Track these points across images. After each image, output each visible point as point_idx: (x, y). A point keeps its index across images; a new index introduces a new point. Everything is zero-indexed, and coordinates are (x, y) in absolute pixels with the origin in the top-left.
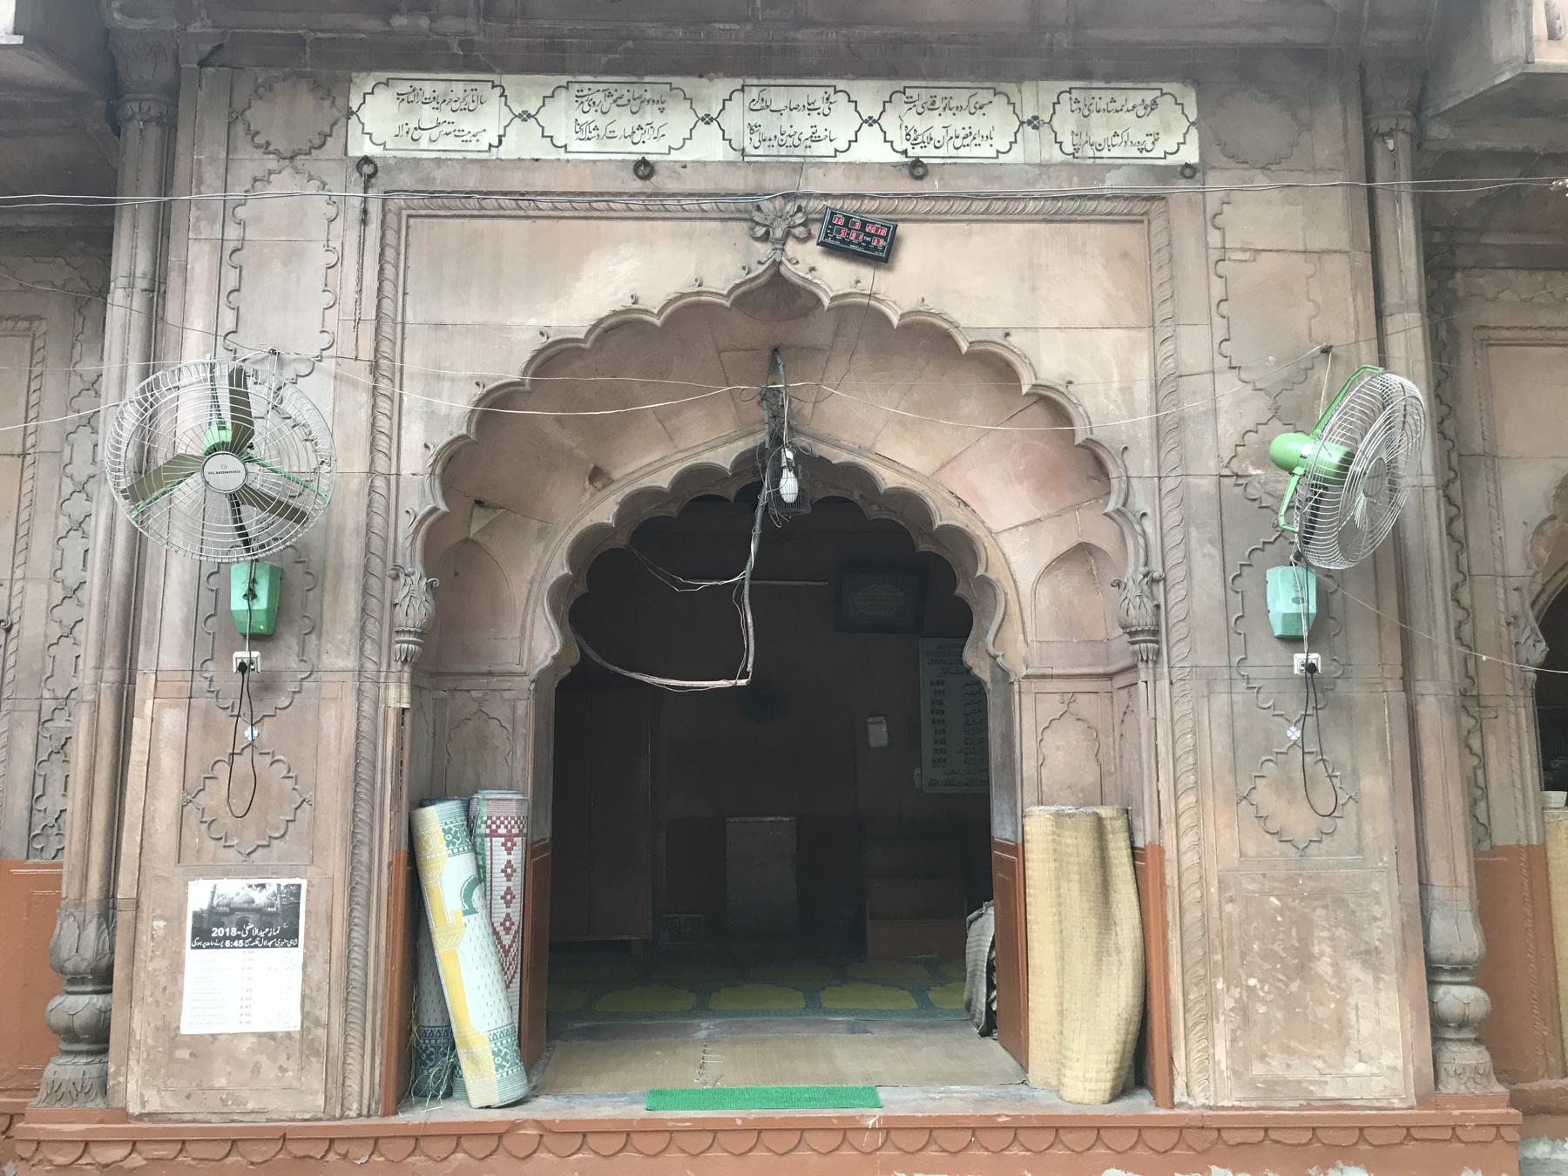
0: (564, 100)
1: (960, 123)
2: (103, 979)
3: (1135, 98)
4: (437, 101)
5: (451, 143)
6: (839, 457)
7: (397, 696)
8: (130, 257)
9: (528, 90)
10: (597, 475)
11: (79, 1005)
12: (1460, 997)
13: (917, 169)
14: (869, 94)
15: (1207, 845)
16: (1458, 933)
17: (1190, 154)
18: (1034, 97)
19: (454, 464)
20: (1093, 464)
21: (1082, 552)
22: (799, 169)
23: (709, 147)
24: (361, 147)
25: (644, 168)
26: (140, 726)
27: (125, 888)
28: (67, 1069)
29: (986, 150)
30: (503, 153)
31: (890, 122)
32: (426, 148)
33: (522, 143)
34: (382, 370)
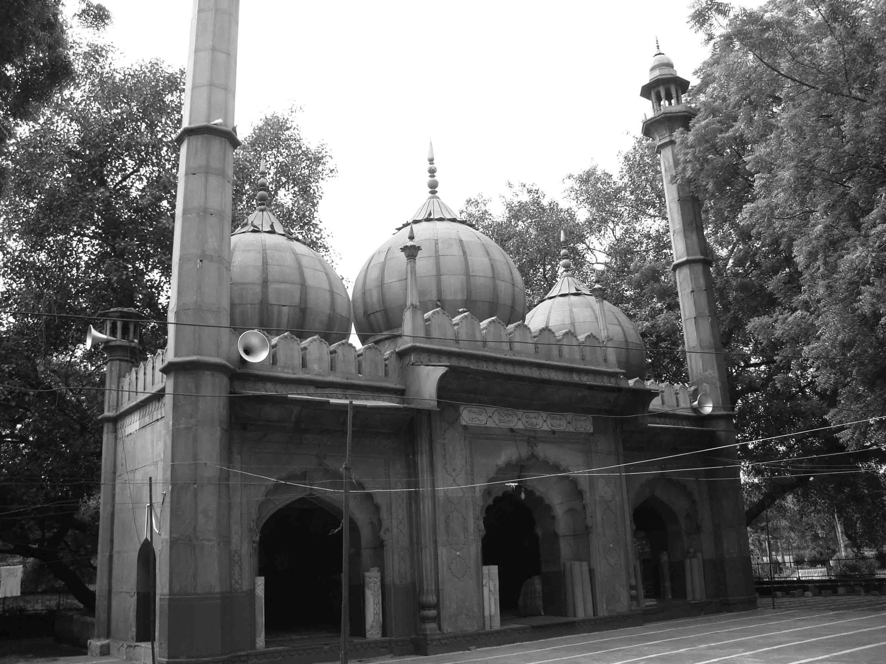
0: (496, 413)
2: (436, 606)
3: (583, 418)
4: (475, 413)
5: (478, 422)
6: (529, 489)
8: (425, 447)
13: (554, 432)
14: (544, 415)
15: (601, 567)
17: (591, 431)
20: (580, 494)
21: (571, 511)
22: (535, 431)
23: (520, 426)
24: (464, 423)
25: (512, 430)
26: (439, 553)
27: (440, 587)
28: (434, 625)
29: (562, 428)
30: (488, 425)
31: (549, 422)
33: (490, 424)
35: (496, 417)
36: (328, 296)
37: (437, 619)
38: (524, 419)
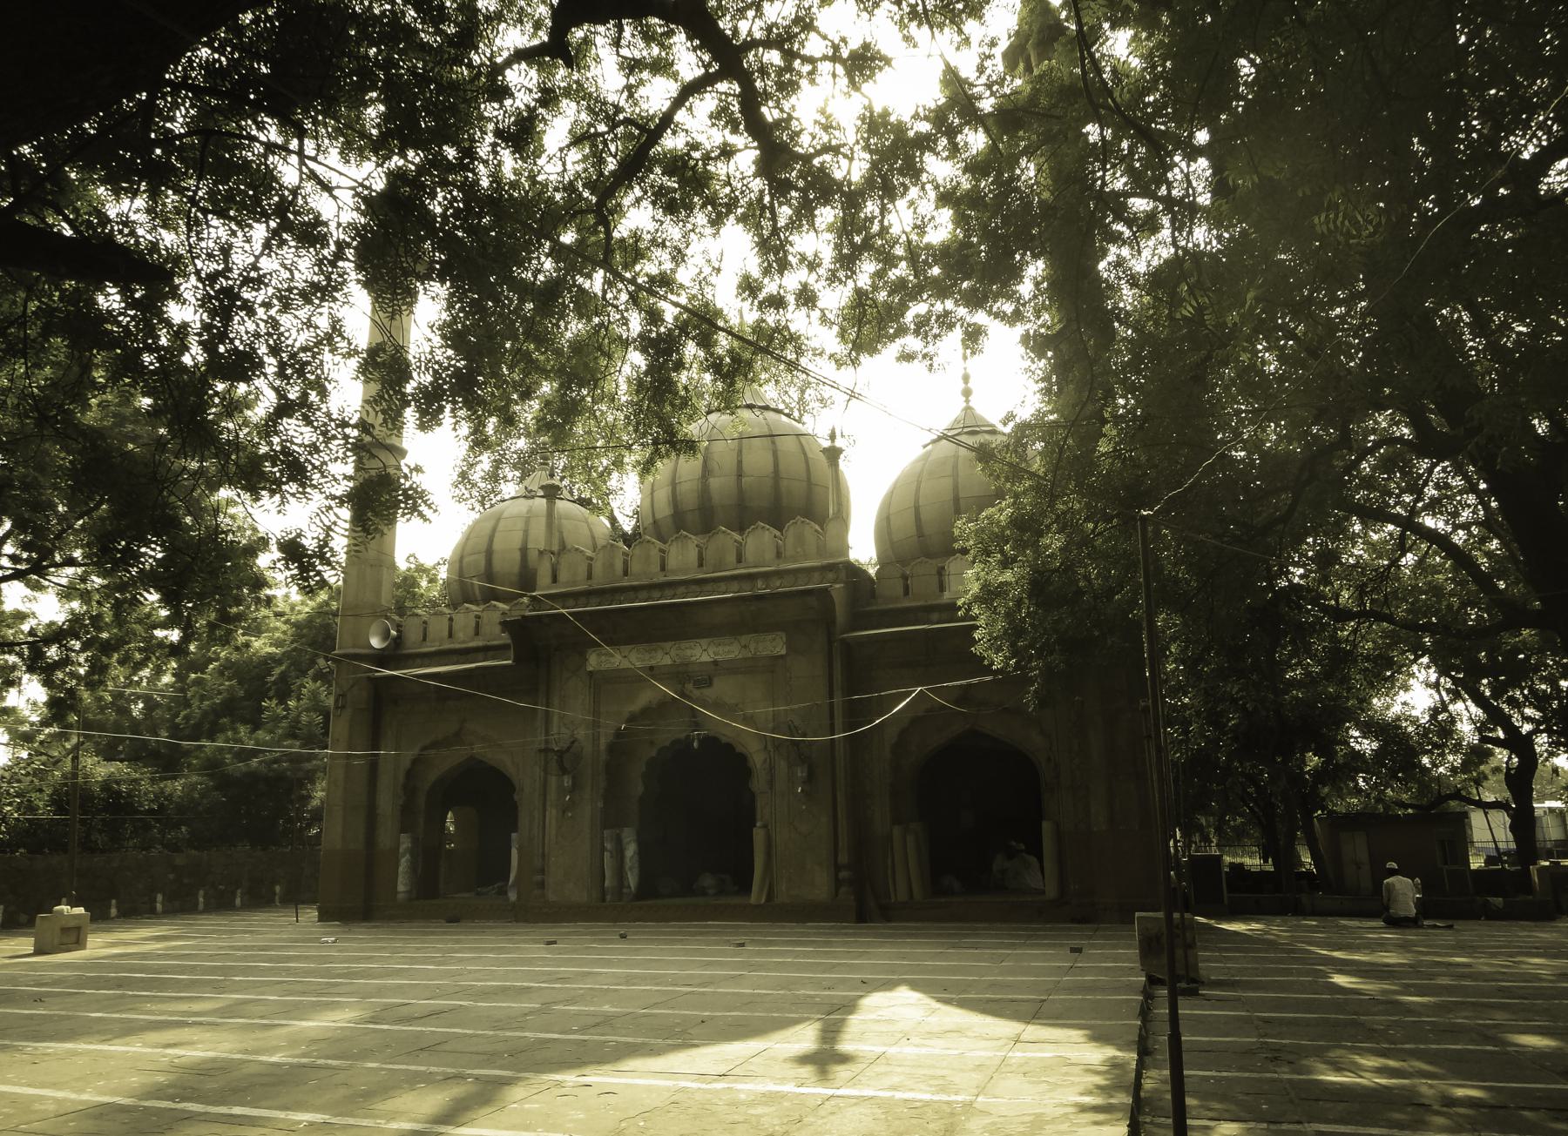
1: (727, 648)
2: (542, 871)
7: (600, 805)
9: (625, 649)
10: (652, 743)
11: (539, 878)
12: (844, 874)
13: (715, 663)
14: (704, 642)
16: (843, 858)
17: (783, 652)
18: (744, 639)
19: (612, 748)
23: (667, 661)
32: (604, 667)
33: (626, 664)
34: (595, 725)
35: (634, 657)
36: (517, 556)
37: (542, 885)
38: (673, 653)
